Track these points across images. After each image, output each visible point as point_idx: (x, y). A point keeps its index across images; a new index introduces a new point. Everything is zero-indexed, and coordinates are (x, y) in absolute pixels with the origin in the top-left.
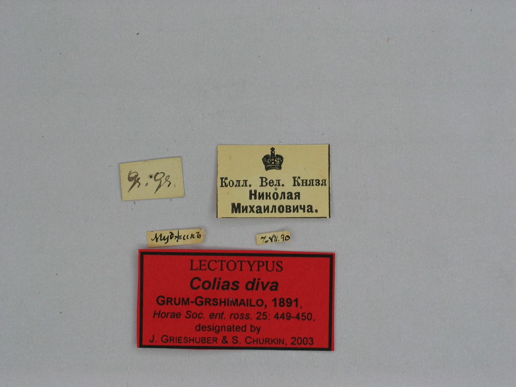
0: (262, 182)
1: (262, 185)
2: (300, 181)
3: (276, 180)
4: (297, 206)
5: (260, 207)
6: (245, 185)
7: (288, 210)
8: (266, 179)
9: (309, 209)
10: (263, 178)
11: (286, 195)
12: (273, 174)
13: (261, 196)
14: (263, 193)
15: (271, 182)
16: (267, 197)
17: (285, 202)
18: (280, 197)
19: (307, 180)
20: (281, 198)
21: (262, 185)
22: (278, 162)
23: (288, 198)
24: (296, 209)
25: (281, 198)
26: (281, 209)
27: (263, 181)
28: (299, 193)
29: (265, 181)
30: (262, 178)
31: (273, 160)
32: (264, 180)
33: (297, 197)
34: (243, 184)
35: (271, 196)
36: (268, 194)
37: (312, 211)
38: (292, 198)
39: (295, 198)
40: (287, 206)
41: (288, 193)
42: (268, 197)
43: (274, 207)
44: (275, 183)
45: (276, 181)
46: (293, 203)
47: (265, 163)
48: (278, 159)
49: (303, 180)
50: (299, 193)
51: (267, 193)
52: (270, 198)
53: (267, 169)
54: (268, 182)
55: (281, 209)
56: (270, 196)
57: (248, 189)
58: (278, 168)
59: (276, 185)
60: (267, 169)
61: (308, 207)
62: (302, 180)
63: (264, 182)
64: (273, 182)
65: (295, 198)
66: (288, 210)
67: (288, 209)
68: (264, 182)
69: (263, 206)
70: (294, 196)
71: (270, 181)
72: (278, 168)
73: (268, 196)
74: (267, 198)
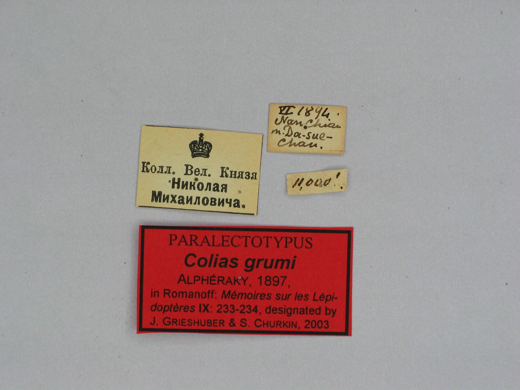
1: (186, 174)
12: (199, 162)
15: (197, 170)
21: (186, 174)
27: (189, 169)
29: (190, 170)
30: (187, 166)
31: (201, 147)
32: (189, 167)
45: (202, 170)
48: (207, 146)
53: (194, 156)
54: (193, 170)
56: (195, 186)
60: (194, 156)
63: (189, 170)
64: (199, 171)
68: (189, 170)
71: (196, 169)
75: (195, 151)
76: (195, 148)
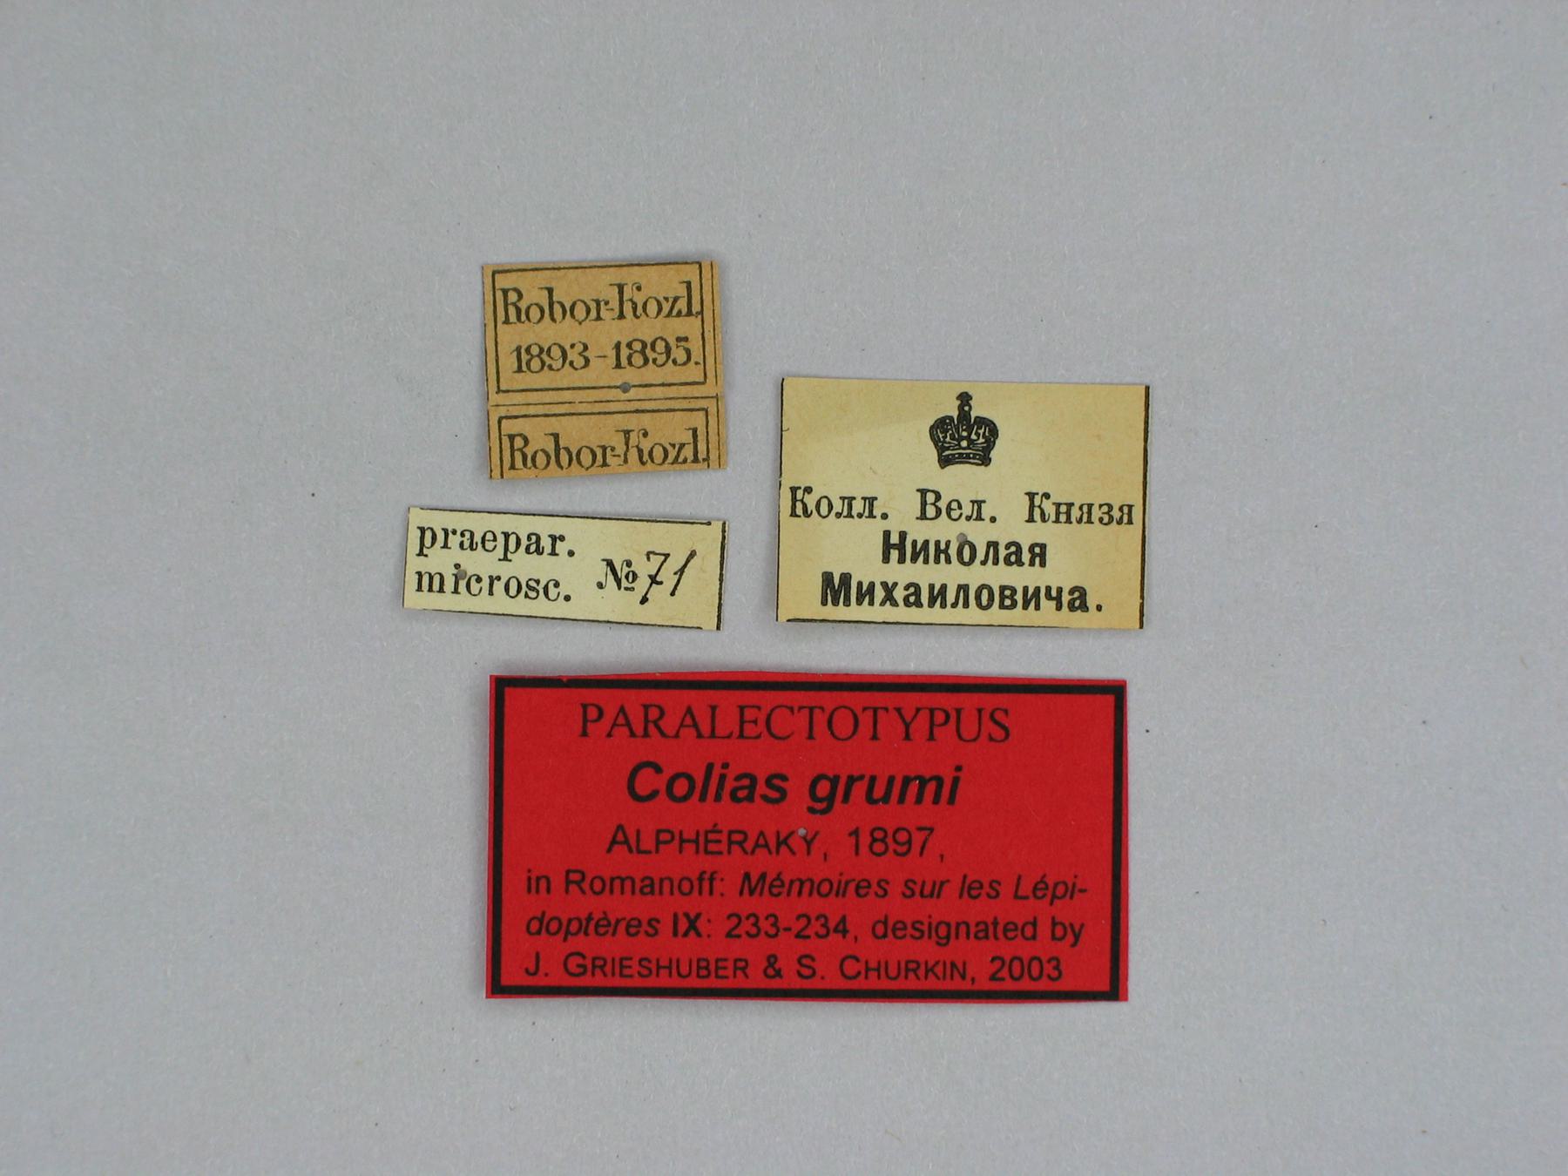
0: (924, 504)
1: (923, 517)
2: (1049, 509)
3: (971, 501)
4: (1038, 589)
5: (917, 587)
6: (867, 514)
7: (1008, 602)
8: (938, 497)
9: (1076, 599)
10: (929, 491)
11: (1002, 553)
12: (960, 482)
13: (920, 552)
14: (926, 543)
15: (954, 505)
16: (939, 557)
17: (998, 575)
18: (980, 555)
19: (1072, 504)
20: (984, 563)
21: (923, 517)
22: (979, 442)
23: (1008, 562)
24: (1032, 598)
25: (984, 563)
26: (985, 597)
27: (928, 502)
28: (1043, 547)
29: (934, 504)
30: (923, 492)
31: (965, 434)
32: (930, 498)
33: (1037, 560)
34: (862, 512)
35: (953, 551)
36: (943, 546)
37: (1084, 607)
38: (1020, 563)
39: (1032, 564)
40: (1003, 588)
41: (1008, 547)
42: (943, 556)
43: (963, 588)
44: (967, 510)
46: (1023, 577)
47: (940, 447)
49: (1058, 505)
50: (1043, 547)
51: (937, 543)
52: (948, 561)
53: (945, 462)
54: (942, 504)
55: (985, 597)
56: (949, 552)
57: (879, 526)
58: (980, 462)
59: (971, 517)
60: (945, 462)
61: (1071, 592)
62: (1054, 504)
63: (932, 504)
65: (1032, 564)
66: (1008, 602)
67: (1007, 597)
68: (932, 504)
69: (927, 587)
70: (1026, 557)
72: (980, 462)
73: (942, 552)
74: (937, 561)
75: (948, 449)
76: (948, 439)
